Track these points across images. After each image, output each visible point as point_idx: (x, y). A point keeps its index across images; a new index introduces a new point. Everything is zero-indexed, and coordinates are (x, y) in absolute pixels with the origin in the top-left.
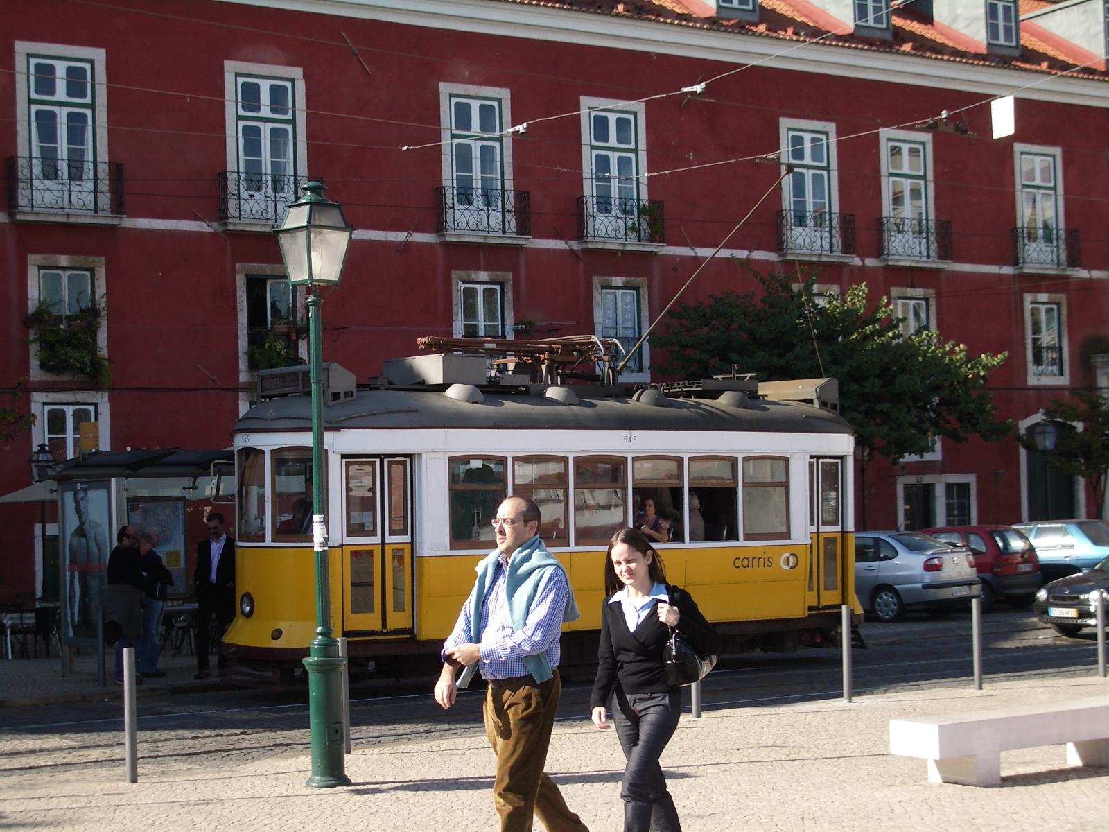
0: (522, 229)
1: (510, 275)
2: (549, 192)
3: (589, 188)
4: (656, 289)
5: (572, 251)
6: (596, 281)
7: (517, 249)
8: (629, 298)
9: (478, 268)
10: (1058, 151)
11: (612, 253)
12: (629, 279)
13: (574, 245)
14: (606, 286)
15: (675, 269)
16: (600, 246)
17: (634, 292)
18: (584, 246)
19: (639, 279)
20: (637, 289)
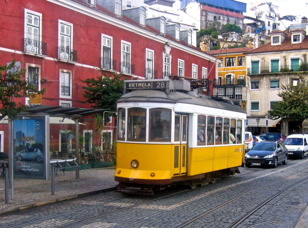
0: (44, 53)
1: (40, 66)
2: (49, 44)
3: (60, 45)
4: (74, 74)
5: (55, 61)
6: (60, 70)
7: (42, 58)
8: (67, 76)
9: (32, 63)
10: (153, 51)
11: (65, 63)
12: (68, 71)
13: (56, 59)
14: (63, 72)
15: (78, 69)
16: (62, 61)
17: (68, 74)
18: (58, 60)
19: (70, 71)
20: (69, 73)
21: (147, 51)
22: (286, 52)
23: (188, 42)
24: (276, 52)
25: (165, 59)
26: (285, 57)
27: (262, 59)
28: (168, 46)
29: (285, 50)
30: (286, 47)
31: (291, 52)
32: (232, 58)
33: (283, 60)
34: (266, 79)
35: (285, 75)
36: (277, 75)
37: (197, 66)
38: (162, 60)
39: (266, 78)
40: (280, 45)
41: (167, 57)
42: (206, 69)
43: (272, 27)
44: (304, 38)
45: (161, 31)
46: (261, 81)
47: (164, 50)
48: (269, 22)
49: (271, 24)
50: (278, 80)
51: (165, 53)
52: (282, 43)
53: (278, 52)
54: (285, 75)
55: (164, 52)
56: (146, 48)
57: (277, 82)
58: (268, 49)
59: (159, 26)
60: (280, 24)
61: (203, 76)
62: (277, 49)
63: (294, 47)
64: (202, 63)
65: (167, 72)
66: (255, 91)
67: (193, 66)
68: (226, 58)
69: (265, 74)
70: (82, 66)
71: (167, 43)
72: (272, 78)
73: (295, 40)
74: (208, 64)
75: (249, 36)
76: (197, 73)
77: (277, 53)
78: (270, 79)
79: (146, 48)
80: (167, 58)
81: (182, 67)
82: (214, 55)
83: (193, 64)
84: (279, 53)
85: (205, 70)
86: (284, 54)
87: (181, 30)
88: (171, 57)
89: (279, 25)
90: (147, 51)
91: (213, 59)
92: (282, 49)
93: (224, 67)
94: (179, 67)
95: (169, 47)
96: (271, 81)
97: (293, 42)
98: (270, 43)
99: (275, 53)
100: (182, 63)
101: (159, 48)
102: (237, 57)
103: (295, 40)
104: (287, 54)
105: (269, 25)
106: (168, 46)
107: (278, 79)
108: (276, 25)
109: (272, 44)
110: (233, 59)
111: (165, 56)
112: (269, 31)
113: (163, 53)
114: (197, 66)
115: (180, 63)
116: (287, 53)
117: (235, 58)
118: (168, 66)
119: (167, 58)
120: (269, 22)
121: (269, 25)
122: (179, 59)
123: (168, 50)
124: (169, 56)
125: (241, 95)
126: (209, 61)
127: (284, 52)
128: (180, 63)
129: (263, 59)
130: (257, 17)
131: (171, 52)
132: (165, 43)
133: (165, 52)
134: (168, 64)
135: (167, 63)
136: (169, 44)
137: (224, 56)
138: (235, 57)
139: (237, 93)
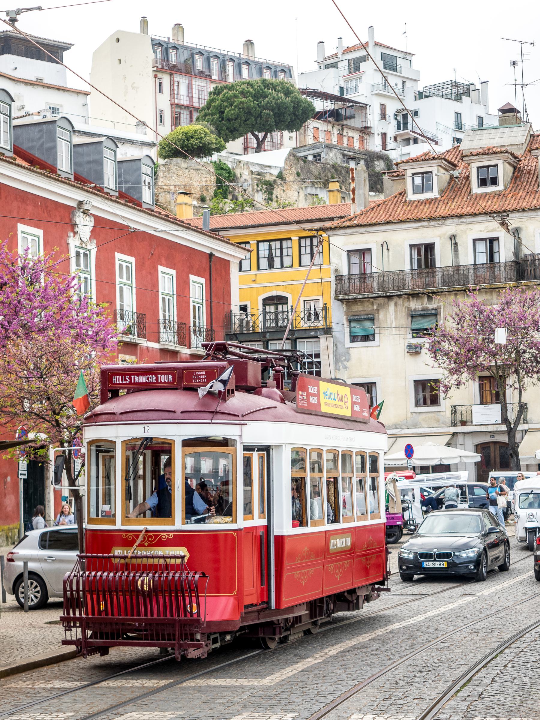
21: (23, 232)
22: (456, 220)
23: (141, 197)
24: (425, 223)
25: (78, 254)
26: (453, 237)
27: (382, 245)
28: (84, 213)
29: (452, 217)
30: (454, 207)
31: (471, 223)
32: (281, 240)
33: (449, 246)
34: (396, 312)
35: (456, 294)
36: (430, 296)
37: (173, 272)
39: (396, 304)
40: (436, 199)
41: (82, 248)
42: (202, 280)
43: (394, 123)
44: (511, 174)
45: (59, 167)
46: (381, 315)
47: (73, 226)
48: (383, 107)
49: (390, 111)
50: (433, 312)
51: (77, 236)
52: (442, 192)
53: (433, 223)
54: (456, 294)
55: (72, 234)
56: (19, 225)
57: (434, 319)
58: (400, 213)
59: (53, 150)
60: (420, 113)
61: (192, 304)
62: (426, 212)
63: (483, 205)
64: (188, 261)
66: (359, 350)
69: (392, 291)
71: (81, 203)
72: (415, 305)
73: (483, 182)
74: (205, 264)
75: (319, 156)
76: (175, 297)
77: (429, 226)
78: (409, 309)
79: (19, 225)
80: (82, 251)
81: (128, 279)
82: (221, 233)
83: (161, 268)
84: (434, 226)
85: (197, 287)
86: (451, 227)
87: (120, 158)
89: (416, 113)
90: (23, 232)
91: (221, 250)
92: (442, 211)
93: (254, 271)
94: (118, 279)
95: (87, 218)
96: (412, 317)
97: (476, 189)
98: (403, 193)
99: (423, 227)
100: (127, 267)
101: (57, 219)
102: (295, 238)
103: (483, 182)
104: (462, 227)
105: (383, 117)
106: (86, 212)
107: (436, 309)
108: (405, 117)
109: (411, 197)
110: (284, 243)
112: (384, 135)
114: (173, 272)
115: (121, 266)
116: (461, 223)
117: (289, 242)
120: (383, 107)
121: (383, 117)
122: (118, 255)
123: (85, 225)
124: (89, 247)
126: (211, 255)
127: (449, 221)
128: (121, 266)
129: (385, 245)
130: (341, 89)
131: (94, 233)
132: (74, 204)
133: (75, 233)
135: (82, 267)
136: (86, 207)
138: (290, 239)
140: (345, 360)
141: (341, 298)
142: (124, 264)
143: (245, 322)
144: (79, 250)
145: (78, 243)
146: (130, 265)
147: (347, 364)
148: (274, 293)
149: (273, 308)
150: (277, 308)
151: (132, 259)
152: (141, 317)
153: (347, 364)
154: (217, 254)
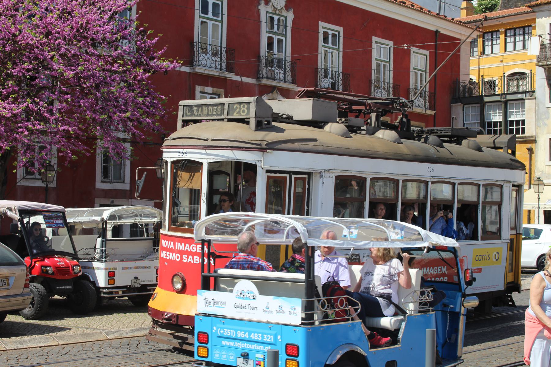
38: (259, 21)
41: (275, 14)
51: (271, 4)
65: (382, 80)
67: (374, 45)
68: (507, 30)
70: (240, 80)
83: (374, 39)
85: (419, 59)
88: (290, 16)
100: (334, 36)
110: (526, 29)
111: (267, 12)
113: (259, 4)
118: (384, 66)
119: (276, 18)
122: (321, 24)
125: (523, 121)
126: (437, 32)
134: (281, 35)
137: (502, 25)
139: (513, 118)
140: (545, 118)
141: (541, 64)
142: (330, 32)
143: (467, 87)
144: (272, 15)
145: (270, 9)
146: (337, 33)
147: (547, 122)
148: (516, 70)
149: (515, 83)
150: (518, 83)
151: (341, 29)
152: (346, 76)
153: (547, 122)
154: (442, 32)
